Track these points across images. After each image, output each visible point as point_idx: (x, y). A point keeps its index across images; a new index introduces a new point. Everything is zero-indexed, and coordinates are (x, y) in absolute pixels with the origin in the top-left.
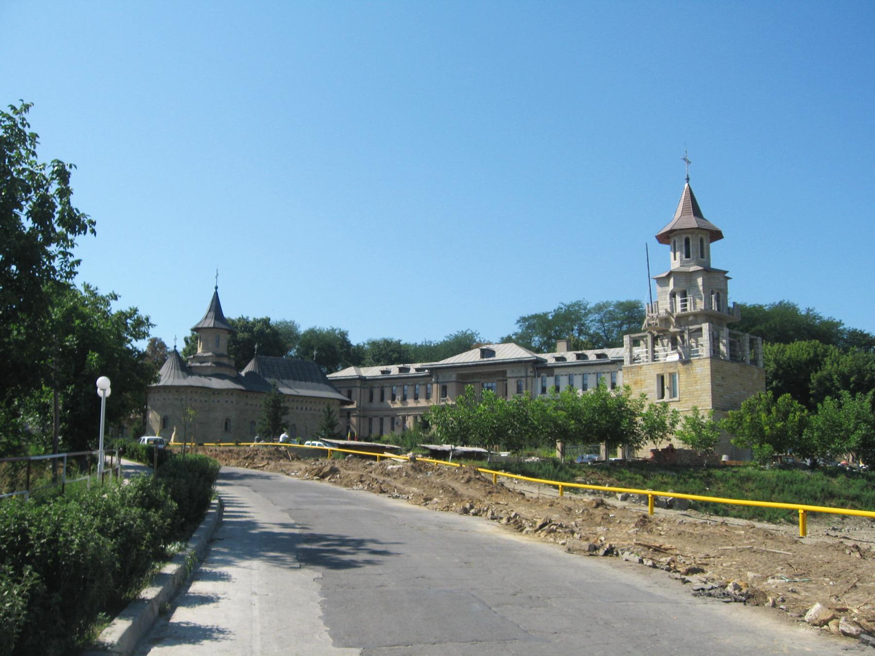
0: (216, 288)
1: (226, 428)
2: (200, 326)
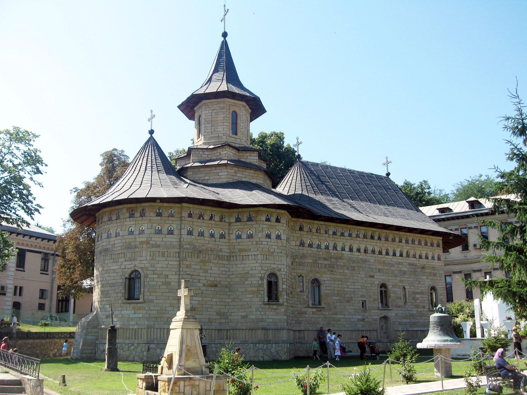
0: (225, 35)
1: (270, 298)
2: (201, 91)
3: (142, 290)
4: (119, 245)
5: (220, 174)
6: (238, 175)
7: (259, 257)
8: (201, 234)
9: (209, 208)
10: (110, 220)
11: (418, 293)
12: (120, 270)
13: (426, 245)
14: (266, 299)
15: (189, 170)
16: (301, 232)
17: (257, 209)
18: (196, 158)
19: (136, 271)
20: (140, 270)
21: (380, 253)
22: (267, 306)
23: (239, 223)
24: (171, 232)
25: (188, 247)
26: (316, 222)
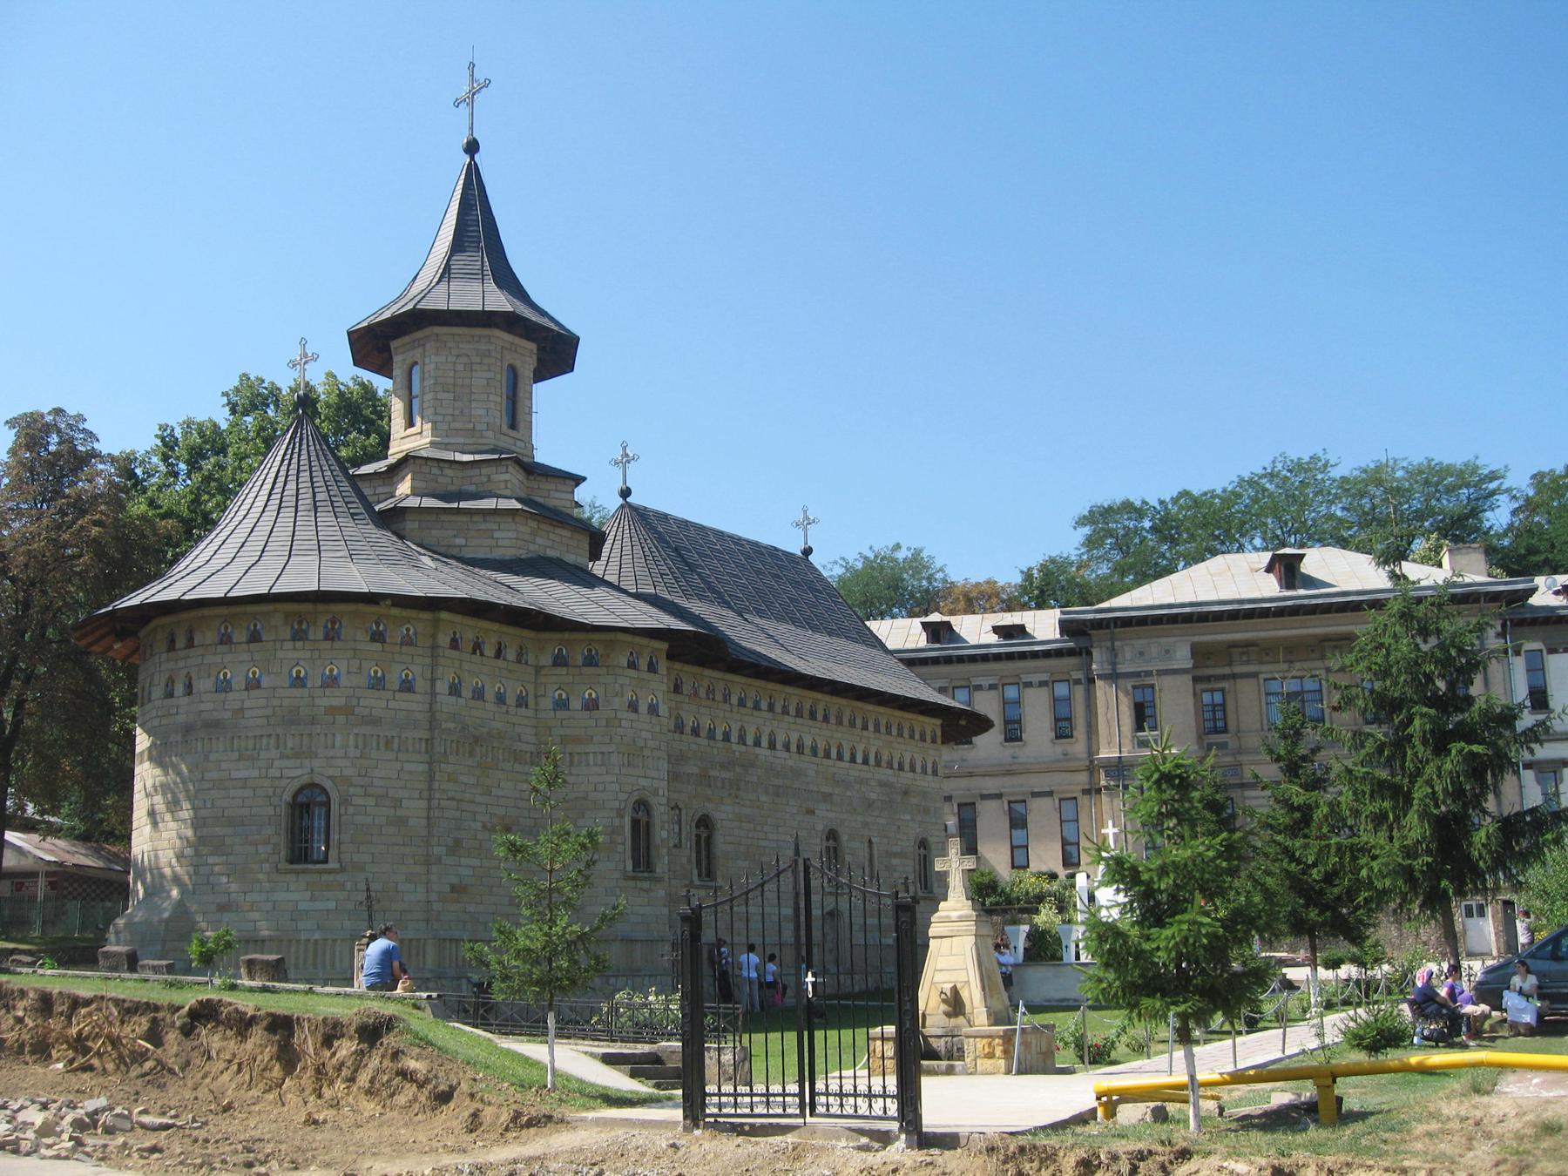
0: (472, 147)
1: (636, 865)
2: (437, 302)
3: (334, 837)
4: (260, 712)
5: (497, 535)
6: (539, 540)
7: (614, 758)
8: (479, 694)
9: (496, 626)
10: (226, 640)
11: (895, 855)
12: (267, 783)
13: (912, 737)
14: (630, 867)
15: (408, 517)
16: (679, 698)
17: (611, 636)
18: (422, 485)
19: (313, 785)
20: (328, 785)
21: (827, 755)
22: (631, 883)
23: (563, 670)
24: (407, 686)
25: (451, 725)
26: (707, 672)
